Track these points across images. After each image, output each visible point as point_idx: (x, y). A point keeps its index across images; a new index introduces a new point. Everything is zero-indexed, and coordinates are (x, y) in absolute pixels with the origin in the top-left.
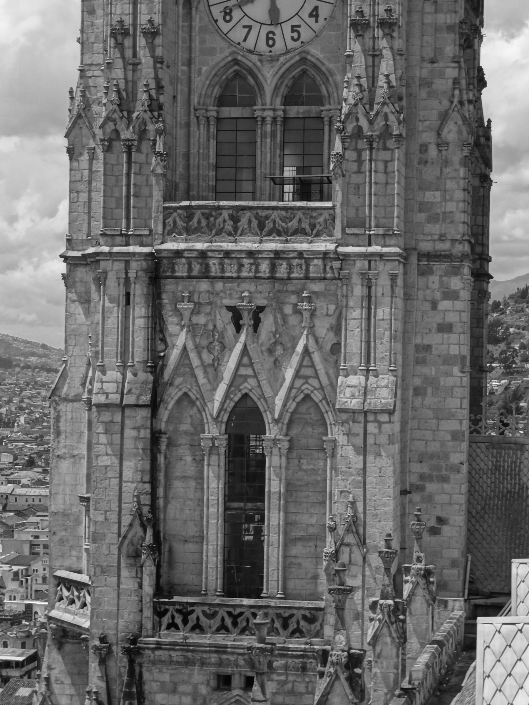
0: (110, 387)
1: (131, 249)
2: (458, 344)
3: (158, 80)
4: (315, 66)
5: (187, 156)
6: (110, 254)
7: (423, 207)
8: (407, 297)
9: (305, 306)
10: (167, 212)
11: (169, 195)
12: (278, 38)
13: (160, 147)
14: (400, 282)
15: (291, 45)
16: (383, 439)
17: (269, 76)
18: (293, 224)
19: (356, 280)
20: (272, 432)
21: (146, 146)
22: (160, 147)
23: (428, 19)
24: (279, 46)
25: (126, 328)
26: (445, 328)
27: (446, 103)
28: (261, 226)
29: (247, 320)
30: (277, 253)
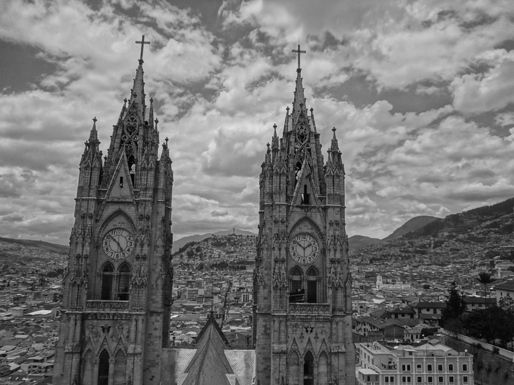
0: (70, 348)
1: (77, 312)
2: (159, 333)
3: (87, 269)
4: (128, 263)
5: (95, 284)
6: (72, 313)
7: (152, 300)
8: (147, 322)
9: (121, 327)
10: (87, 303)
11: (89, 298)
12: (119, 256)
13: (86, 286)
14: (145, 321)
15: (123, 258)
16: (138, 361)
17: (116, 265)
18: (119, 306)
19: (134, 320)
20: (112, 359)
21: (83, 286)
22: (86, 286)
23: (155, 255)
24: (119, 258)
25: (75, 332)
26: (156, 329)
27: (158, 275)
28: (111, 307)
29: (106, 330)
30: (114, 314)
